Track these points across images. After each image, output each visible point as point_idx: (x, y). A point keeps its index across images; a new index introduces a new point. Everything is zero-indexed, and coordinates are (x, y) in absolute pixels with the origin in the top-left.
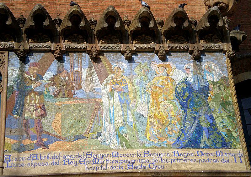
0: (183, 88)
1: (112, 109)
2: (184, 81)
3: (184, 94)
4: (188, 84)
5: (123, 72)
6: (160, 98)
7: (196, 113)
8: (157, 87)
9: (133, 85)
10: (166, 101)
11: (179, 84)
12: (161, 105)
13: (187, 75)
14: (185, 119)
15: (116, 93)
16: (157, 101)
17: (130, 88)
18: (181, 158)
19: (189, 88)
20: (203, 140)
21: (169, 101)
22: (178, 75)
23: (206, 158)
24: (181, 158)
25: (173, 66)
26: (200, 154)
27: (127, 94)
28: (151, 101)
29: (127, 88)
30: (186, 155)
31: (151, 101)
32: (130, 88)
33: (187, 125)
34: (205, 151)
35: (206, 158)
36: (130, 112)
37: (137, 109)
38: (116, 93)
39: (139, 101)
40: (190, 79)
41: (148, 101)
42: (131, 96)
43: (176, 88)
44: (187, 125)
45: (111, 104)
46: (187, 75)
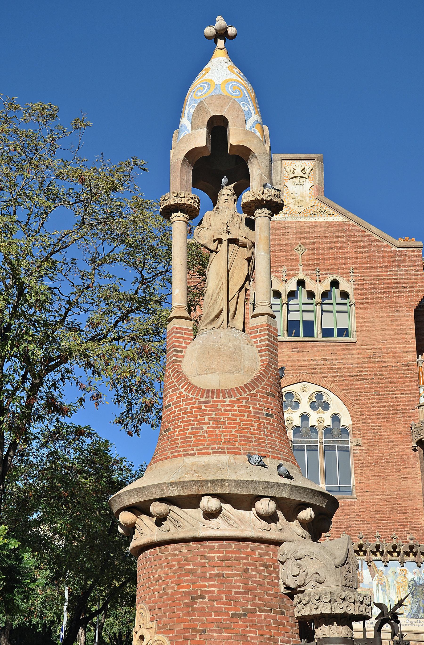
0: (412, 584)
1: (378, 595)
2: (413, 579)
3: (412, 588)
4: (415, 581)
5: (383, 573)
6: (401, 590)
7: (418, 599)
8: (399, 583)
9: (388, 581)
10: (404, 591)
11: (410, 581)
12: (401, 593)
13: (414, 576)
14: (412, 602)
15: (379, 585)
16: (399, 591)
17: (386, 582)
18: (410, 623)
19: (415, 584)
20: (420, 615)
21: (405, 591)
22: (410, 576)
23: (421, 624)
24: (410, 623)
25: (408, 570)
26: (419, 621)
27: (385, 586)
28: (396, 591)
29: (385, 583)
30: (412, 622)
31: (396, 591)
32: (386, 582)
33: (414, 605)
34: (421, 620)
35: (421, 624)
36: (386, 597)
37: (390, 596)
38: (379, 585)
39: (391, 591)
40: (416, 579)
41: (395, 590)
42: (387, 588)
43: (409, 584)
44: (414, 605)
45: (378, 592)
46: (414, 576)
